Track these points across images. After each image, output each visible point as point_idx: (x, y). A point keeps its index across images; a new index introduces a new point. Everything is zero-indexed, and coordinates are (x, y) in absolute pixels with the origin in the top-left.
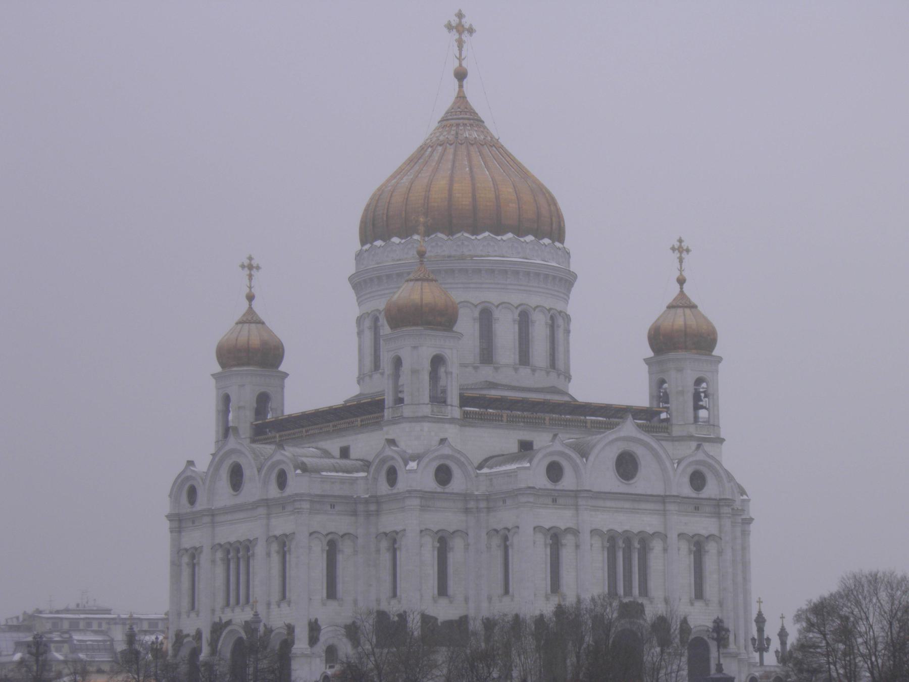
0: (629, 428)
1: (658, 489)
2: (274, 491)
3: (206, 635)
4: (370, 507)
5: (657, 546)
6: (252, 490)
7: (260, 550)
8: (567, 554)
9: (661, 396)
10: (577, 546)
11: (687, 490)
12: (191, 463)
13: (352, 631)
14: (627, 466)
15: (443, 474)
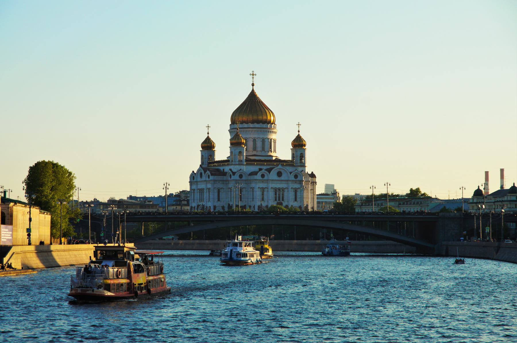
0: (280, 166)
1: (286, 179)
2: (207, 179)
3: (196, 207)
4: (226, 182)
5: (286, 190)
6: (204, 178)
7: (205, 191)
8: (265, 193)
9: (293, 157)
10: (268, 191)
11: (293, 179)
12: (193, 172)
13: (223, 207)
14: (279, 174)
15: (241, 176)
